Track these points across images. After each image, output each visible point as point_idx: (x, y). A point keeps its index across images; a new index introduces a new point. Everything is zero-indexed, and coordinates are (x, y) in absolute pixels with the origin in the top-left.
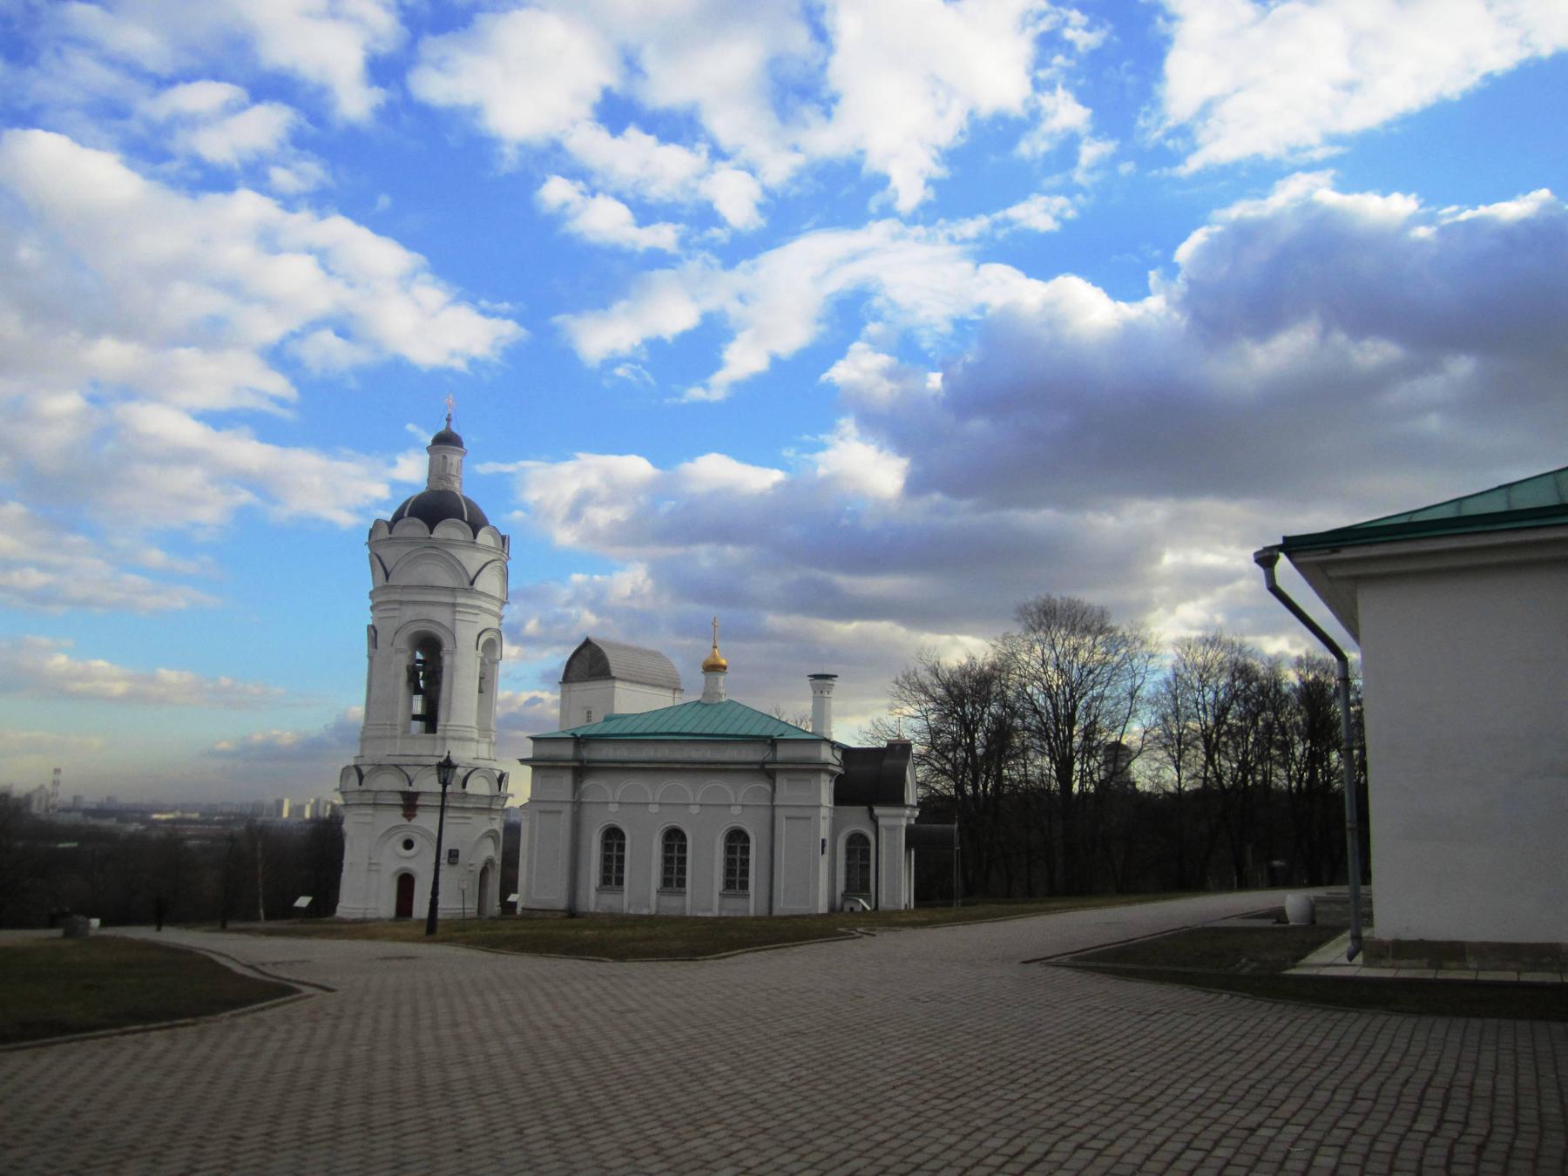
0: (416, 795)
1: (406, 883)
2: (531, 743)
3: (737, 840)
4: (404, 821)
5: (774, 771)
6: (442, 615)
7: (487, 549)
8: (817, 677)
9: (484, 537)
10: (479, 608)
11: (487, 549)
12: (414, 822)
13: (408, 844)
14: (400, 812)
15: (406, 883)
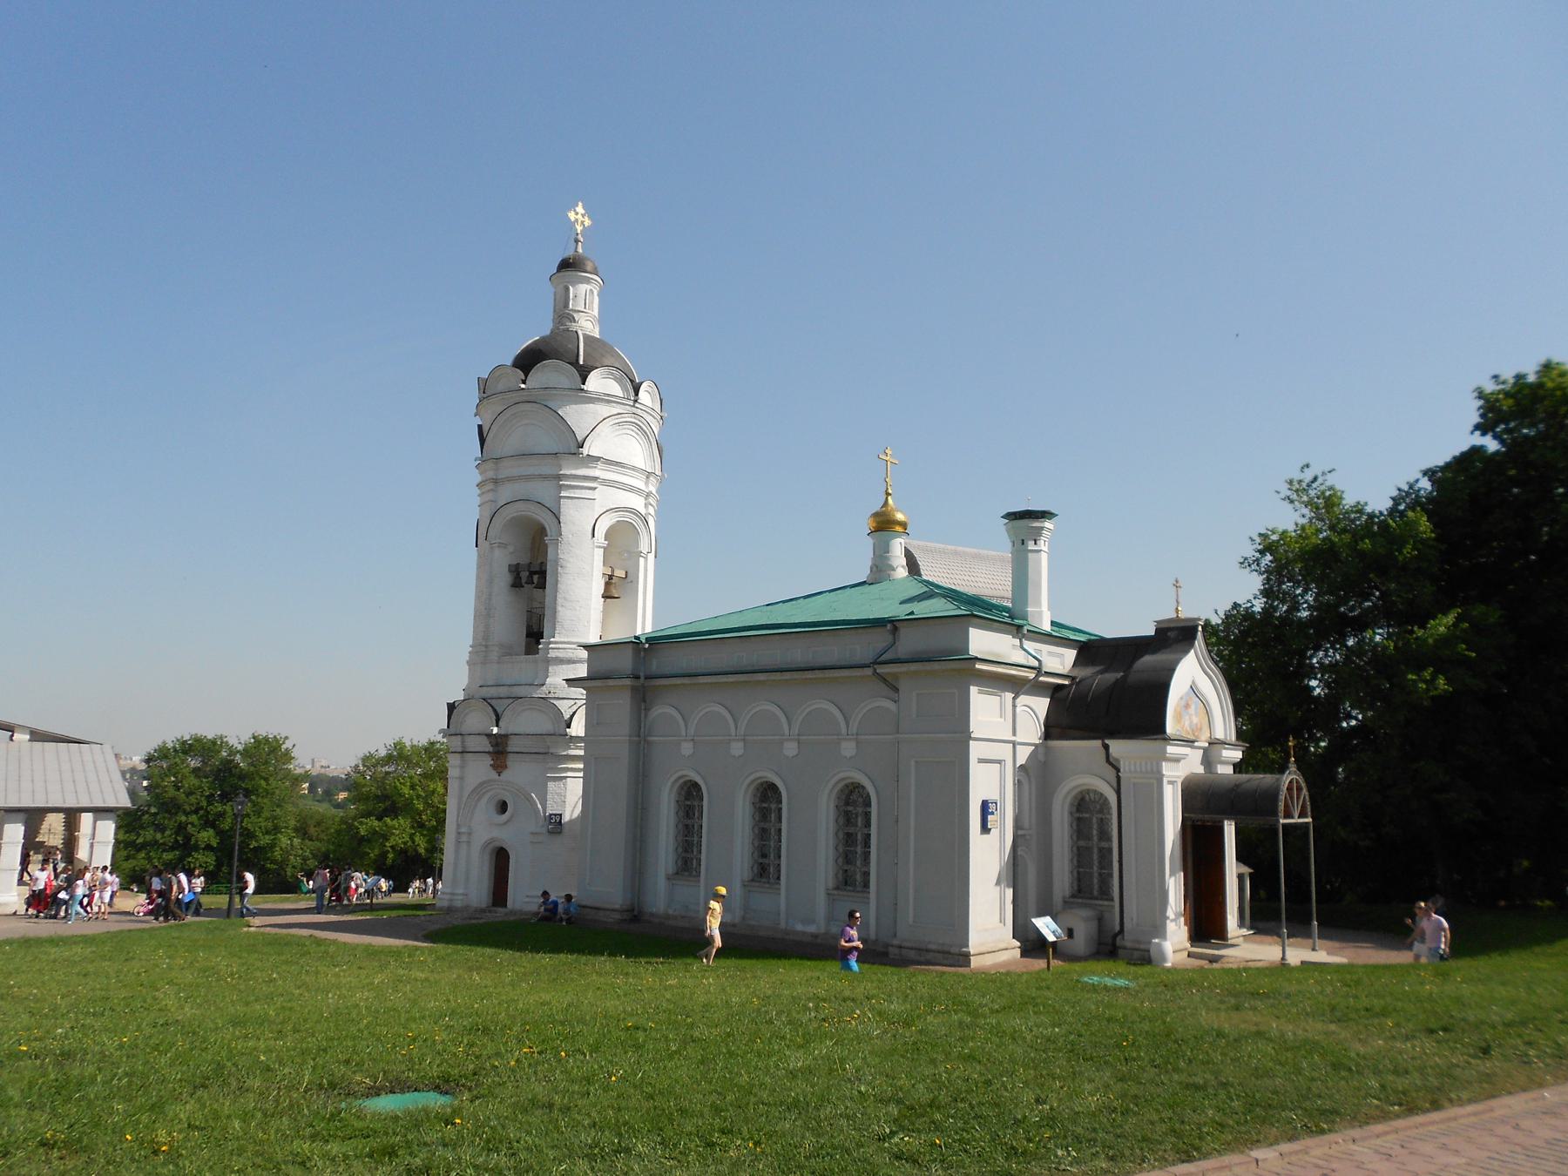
0: (506, 736)
1: (501, 858)
2: (584, 654)
3: (852, 801)
4: (494, 775)
5: (896, 676)
6: (541, 491)
7: (606, 399)
8: (1014, 516)
9: (597, 382)
10: (595, 479)
11: (606, 399)
12: (506, 775)
13: (503, 807)
14: (488, 761)
15: (501, 858)
